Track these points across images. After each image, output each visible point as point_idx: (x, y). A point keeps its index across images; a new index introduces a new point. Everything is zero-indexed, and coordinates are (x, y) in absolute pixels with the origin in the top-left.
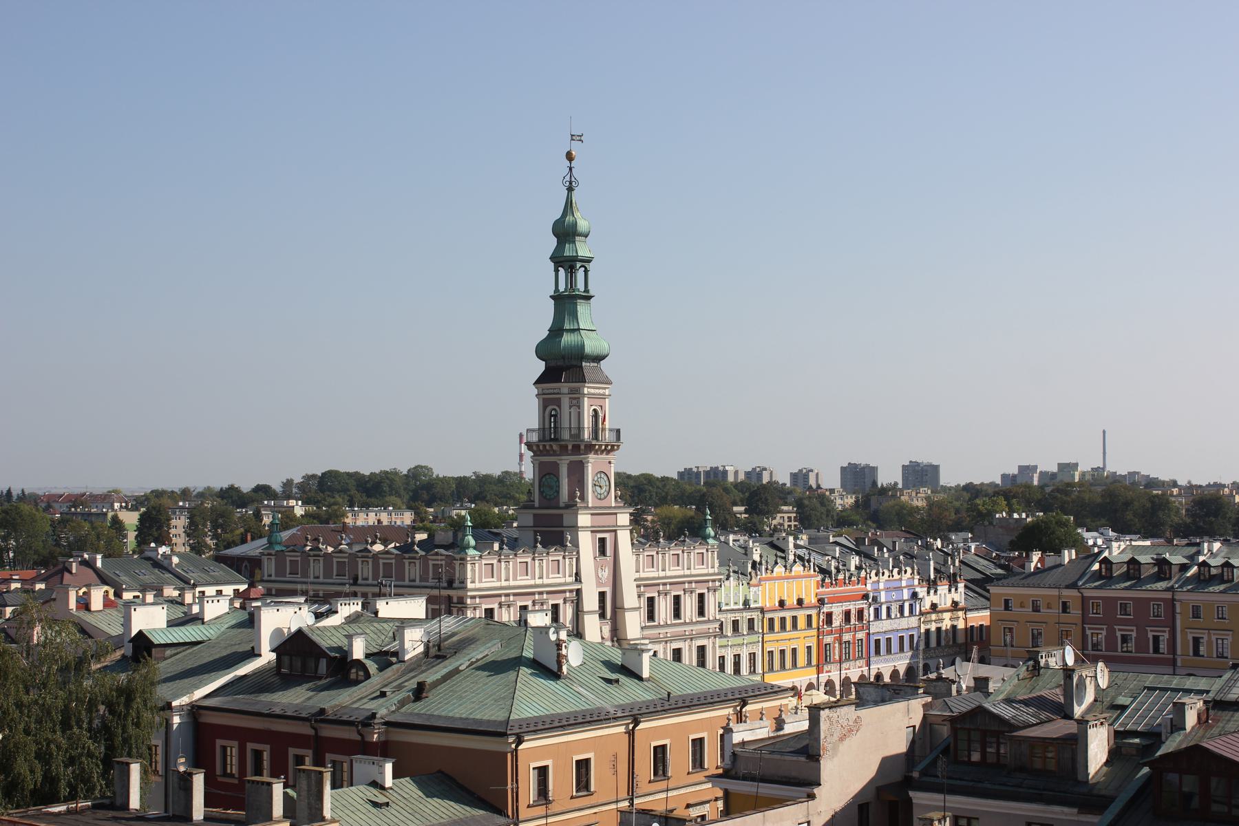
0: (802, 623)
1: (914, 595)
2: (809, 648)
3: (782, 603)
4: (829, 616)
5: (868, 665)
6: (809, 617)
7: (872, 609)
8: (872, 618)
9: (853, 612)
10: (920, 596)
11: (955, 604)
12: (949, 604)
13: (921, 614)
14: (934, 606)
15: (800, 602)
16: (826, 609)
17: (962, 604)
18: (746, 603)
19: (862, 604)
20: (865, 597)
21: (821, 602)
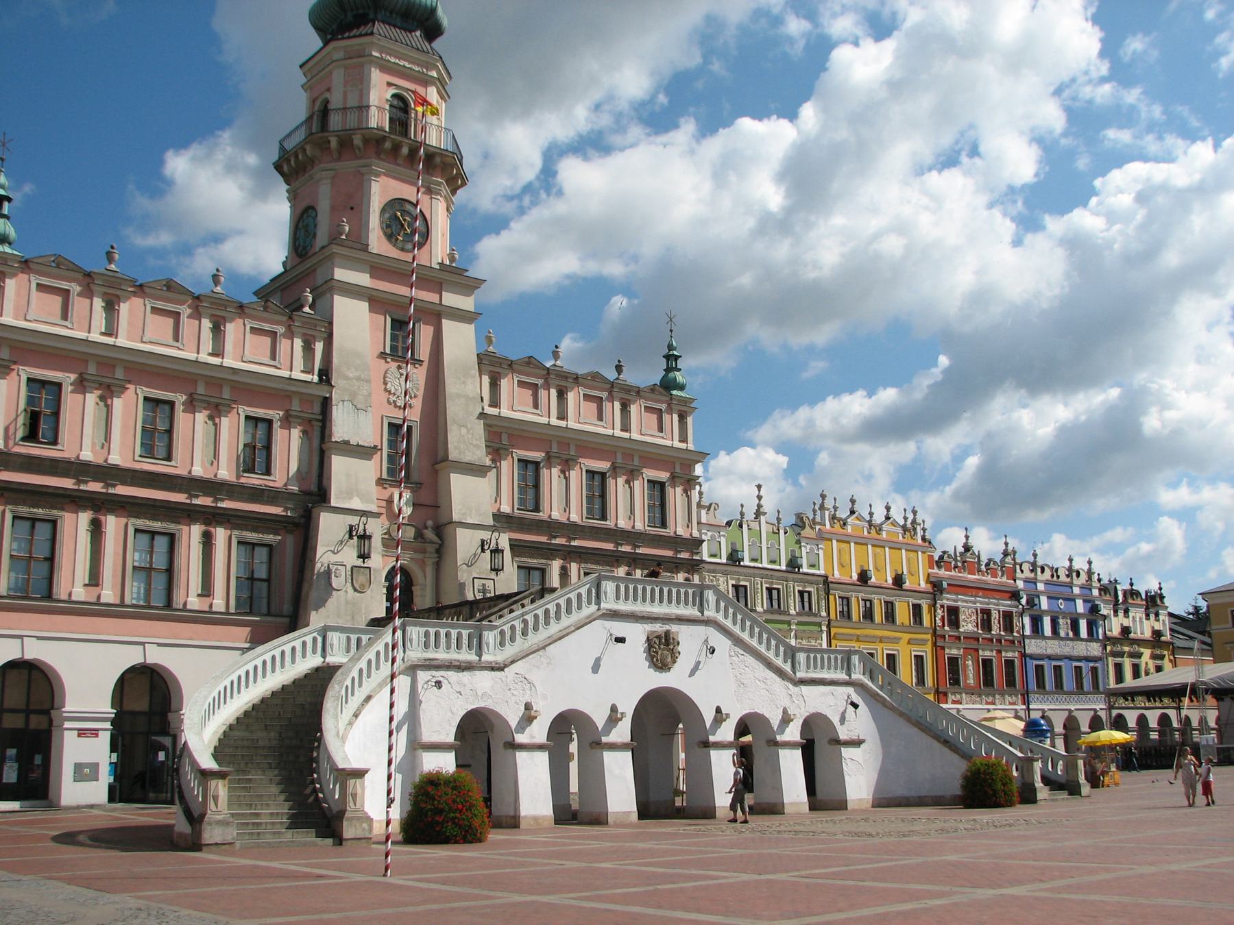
0: (903, 614)
1: (1094, 609)
2: (919, 660)
3: (864, 577)
4: (953, 614)
5: (1026, 702)
6: (917, 609)
7: (1027, 620)
8: (1028, 632)
9: (995, 615)
10: (1104, 611)
11: (1157, 634)
12: (1148, 634)
13: (1106, 638)
14: (1126, 631)
15: (898, 581)
16: (947, 600)
17: (1167, 637)
18: (793, 564)
19: (1006, 605)
20: (1015, 595)
21: (937, 587)
